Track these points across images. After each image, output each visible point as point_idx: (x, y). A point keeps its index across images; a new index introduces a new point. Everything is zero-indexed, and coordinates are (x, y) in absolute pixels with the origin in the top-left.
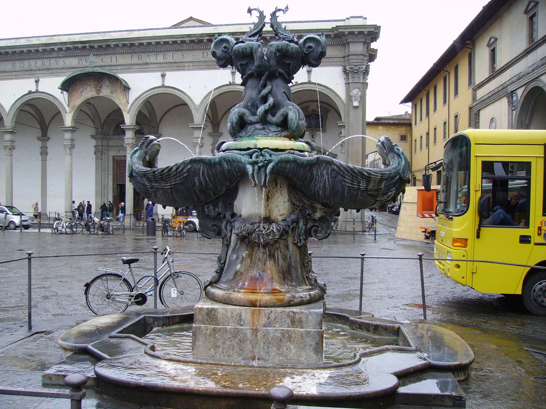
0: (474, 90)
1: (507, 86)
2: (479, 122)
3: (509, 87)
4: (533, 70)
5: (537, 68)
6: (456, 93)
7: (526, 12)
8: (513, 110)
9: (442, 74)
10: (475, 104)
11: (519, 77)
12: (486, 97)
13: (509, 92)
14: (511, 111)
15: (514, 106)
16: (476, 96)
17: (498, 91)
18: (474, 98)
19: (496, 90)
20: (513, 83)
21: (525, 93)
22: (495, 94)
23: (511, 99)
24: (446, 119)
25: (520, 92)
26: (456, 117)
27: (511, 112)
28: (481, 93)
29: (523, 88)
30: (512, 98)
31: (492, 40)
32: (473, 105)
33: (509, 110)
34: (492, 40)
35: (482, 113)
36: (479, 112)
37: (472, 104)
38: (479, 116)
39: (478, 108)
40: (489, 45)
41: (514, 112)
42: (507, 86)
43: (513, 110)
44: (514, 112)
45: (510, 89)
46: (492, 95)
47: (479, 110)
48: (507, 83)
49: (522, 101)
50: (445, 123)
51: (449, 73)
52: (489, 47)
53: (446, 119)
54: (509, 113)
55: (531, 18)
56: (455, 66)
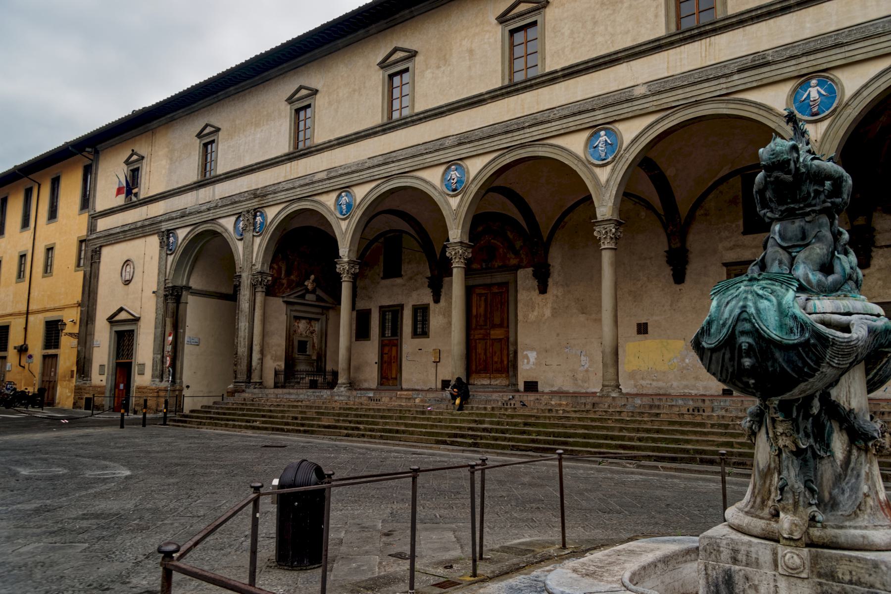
0: (93, 218)
1: (161, 222)
2: (99, 262)
3: (163, 224)
4: (209, 209)
5: (216, 207)
6: (53, 214)
7: (199, 136)
8: (167, 254)
9: (25, 183)
10: (94, 236)
11: (184, 214)
12: (118, 230)
13: (163, 230)
14: (164, 255)
15: (171, 250)
16: (96, 226)
17: (143, 227)
18: (92, 228)
19: (139, 224)
20: (172, 219)
21: (191, 236)
22: (136, 228)
23: (165, 239)
24: (27, 250)
25: (182, 234)
26: (50, 250)
27: (164, 258)
28: (103, 224)
29: (188, 229)
30: (168, 238)
31: (135, 157)
32: (90, 238)
33: (160, 253)
34: (135, 157)
35: (105, 251)
36: (100, 251)
37: (87, 236)
38: (100, 254)
39: (99, 243)
40: (127, 162)
41: (170, 258)
42: (161, 222)
43: (167, 254)
44: (170, 258)
45: (165, 226)
46: (129, 230)
47: (101, 247)
48: (160, 218)
49: (184, 244)
50: (23, 256)
51: (39, 185)
52: (127, 165)
53: (27, 250)
54: (160, 258)
55: (206, 145)
56: (54, 176)
